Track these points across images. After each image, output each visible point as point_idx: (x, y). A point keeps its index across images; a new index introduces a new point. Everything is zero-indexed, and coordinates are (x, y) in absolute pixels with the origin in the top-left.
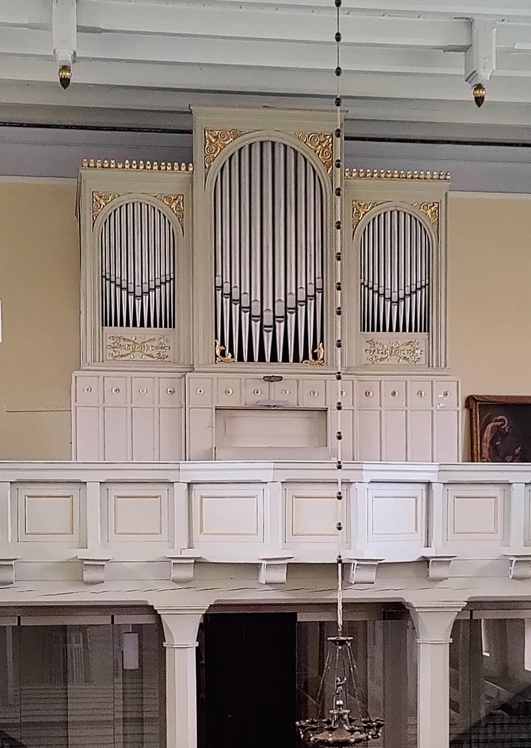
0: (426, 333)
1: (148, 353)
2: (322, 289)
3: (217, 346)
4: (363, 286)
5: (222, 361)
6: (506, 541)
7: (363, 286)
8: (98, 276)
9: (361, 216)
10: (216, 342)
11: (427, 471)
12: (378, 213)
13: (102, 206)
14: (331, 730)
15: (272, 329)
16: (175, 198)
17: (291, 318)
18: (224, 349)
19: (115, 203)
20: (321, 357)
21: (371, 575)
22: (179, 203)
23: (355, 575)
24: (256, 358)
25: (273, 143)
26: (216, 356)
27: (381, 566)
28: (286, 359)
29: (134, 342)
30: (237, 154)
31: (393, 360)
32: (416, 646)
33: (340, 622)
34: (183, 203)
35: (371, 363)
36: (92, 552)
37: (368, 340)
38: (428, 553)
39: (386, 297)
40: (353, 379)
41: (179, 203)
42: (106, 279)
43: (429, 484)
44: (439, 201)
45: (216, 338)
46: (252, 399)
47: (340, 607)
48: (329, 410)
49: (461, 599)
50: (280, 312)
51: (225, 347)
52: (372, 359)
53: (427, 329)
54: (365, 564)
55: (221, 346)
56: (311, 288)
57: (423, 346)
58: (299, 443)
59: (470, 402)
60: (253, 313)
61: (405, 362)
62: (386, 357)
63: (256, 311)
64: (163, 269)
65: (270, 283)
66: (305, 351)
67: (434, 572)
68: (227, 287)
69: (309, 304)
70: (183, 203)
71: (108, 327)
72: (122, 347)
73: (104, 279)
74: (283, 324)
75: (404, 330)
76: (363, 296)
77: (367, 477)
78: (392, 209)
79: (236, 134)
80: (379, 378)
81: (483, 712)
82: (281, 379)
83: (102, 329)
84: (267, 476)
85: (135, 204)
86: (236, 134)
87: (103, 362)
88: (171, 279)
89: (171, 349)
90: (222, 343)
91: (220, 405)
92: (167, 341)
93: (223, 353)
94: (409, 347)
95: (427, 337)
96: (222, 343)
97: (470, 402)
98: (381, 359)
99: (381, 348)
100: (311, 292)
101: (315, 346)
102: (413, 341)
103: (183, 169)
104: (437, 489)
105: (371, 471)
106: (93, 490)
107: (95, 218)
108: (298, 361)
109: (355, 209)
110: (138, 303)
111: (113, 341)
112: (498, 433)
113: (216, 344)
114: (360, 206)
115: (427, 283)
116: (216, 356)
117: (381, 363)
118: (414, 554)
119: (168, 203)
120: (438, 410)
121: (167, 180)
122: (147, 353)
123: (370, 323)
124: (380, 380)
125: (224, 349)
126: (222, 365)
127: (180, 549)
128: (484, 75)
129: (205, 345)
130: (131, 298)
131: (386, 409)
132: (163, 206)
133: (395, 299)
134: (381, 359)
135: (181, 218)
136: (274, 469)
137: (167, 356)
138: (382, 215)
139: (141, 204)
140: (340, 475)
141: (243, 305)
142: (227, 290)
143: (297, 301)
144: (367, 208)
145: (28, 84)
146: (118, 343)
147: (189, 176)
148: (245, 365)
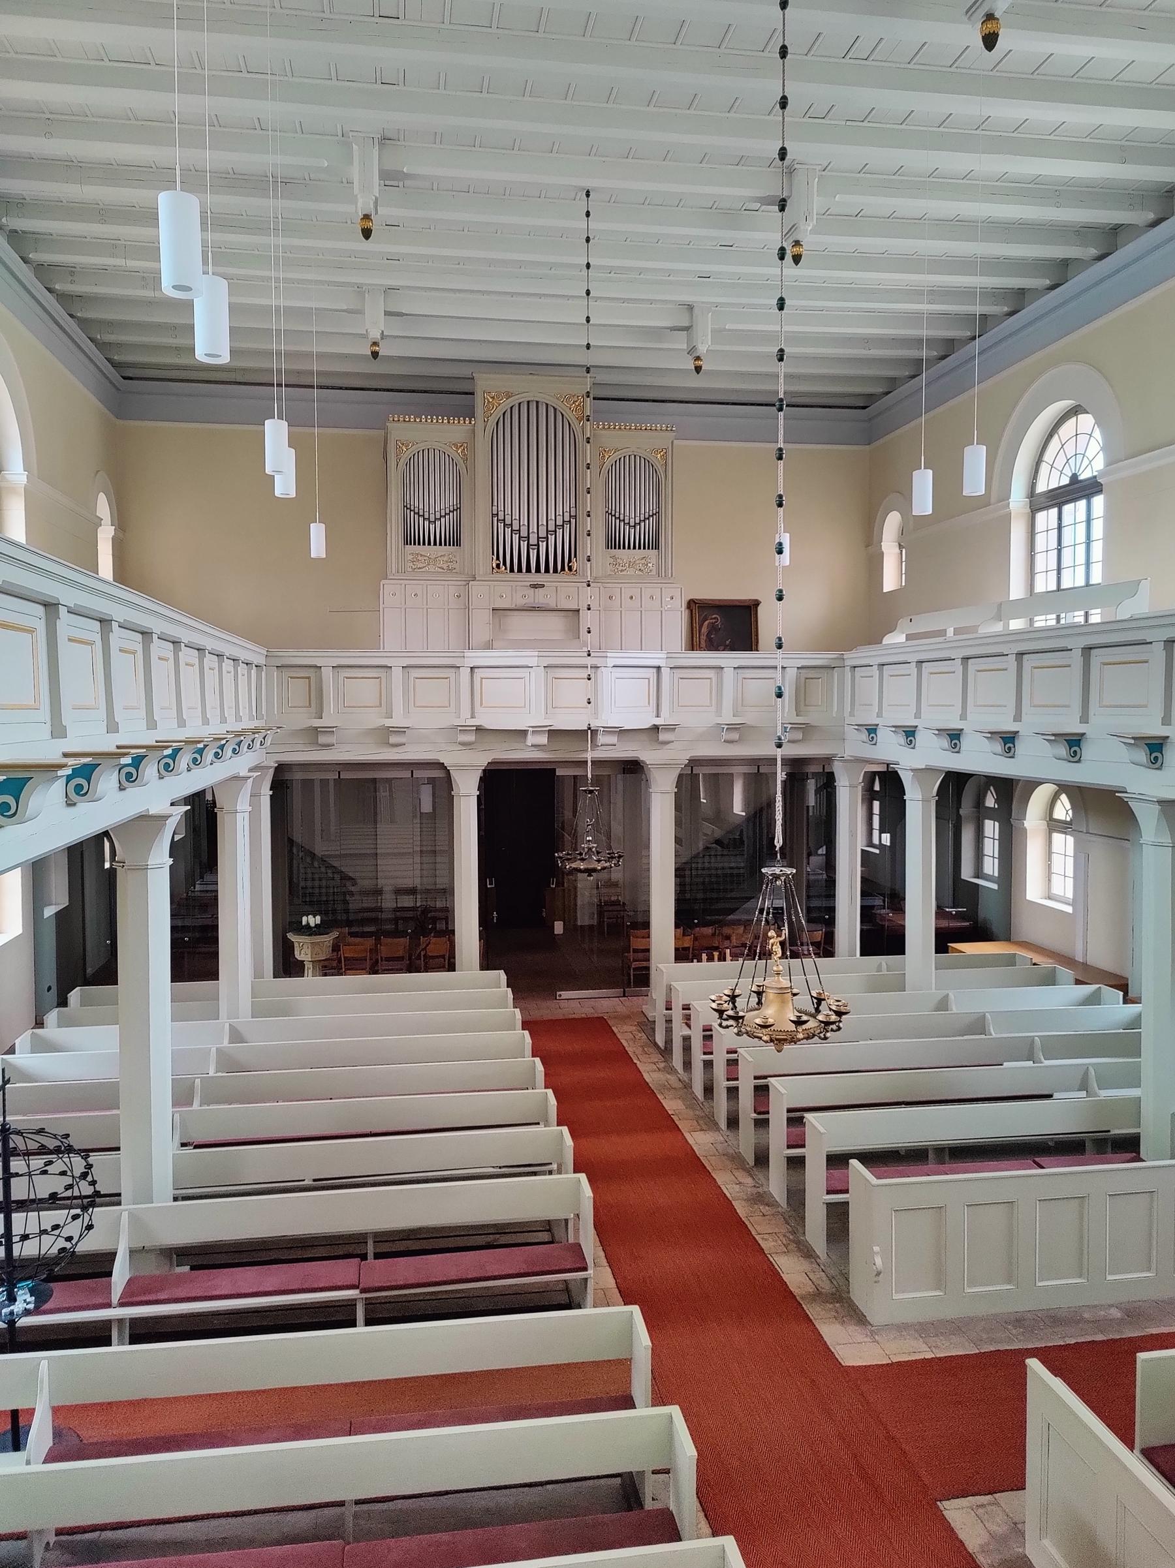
6: (719, 712)
8: (401, 506)
11: (657, 658)
14: (583, 860)
17: (551, 538)
21: (613, 739)
23: (602, 739)
24: (524, 570)
27: (622, 732)
31: (631, 572)
32: (648, 795)
33: (590, 776)
34: (468, 447)
36: (397, 721)
38: (658, 721)
43: (659, 668)
46: (520, 602)
47: (589, 764)
49: (684, 757)
50: (543, 534)
53: (657, 548)
54: (609, 731)
57: (654, 561)
58: (557, 636)
59: (691, 604)
63: (524, 533)
64: (452, 501)
65: (536, 512)
66: (563, 564)
67: (663, 736)
70: (468, 447)
76: (607, 521)
77: (611, 662)
81: (701, 846)
84: (533, 662)
90: (498, 558)
91: (496, 606)
96: (498, 558)
97: (691, 604)
100: (567, 519)
101: (570, 561)
104: (665, 672)
105: (614, 657)
106: (397, 673)
112: (713, 628)
118: (646, 720)
123: (613, 543)
126: (498, 575)
127: (465, 719)
129: (484, 559)
130: (427, 523)
132: (451, 451)
140: (589, 661)
145: (346, 357)
148: (516, 575)
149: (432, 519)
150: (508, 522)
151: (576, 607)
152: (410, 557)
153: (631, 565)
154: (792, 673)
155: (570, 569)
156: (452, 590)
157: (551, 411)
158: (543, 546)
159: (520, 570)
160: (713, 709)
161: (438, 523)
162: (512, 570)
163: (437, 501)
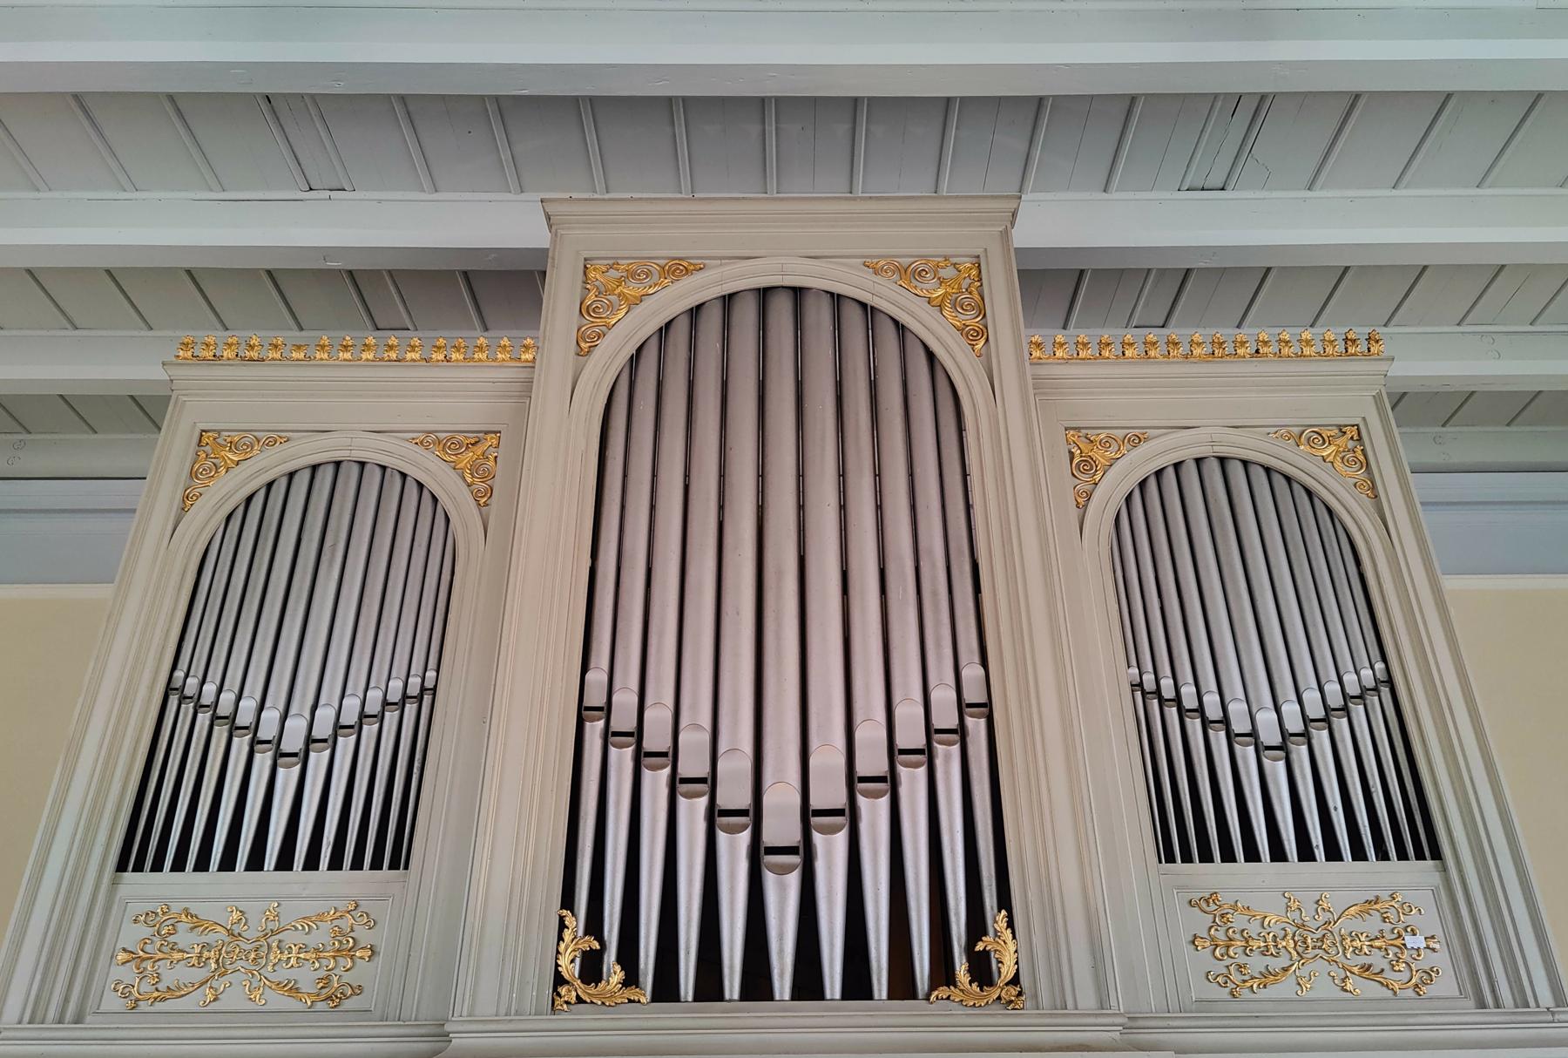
1: (283, 974)
2: (988, 705)
3: (567, 935)
5: (580, 1000)
10: (562, 919)
15: (796, 859)
17: (874, 813)
18: (596, 946)
19: (269, 464)
20: (1008, 971)
24: (732, 982)
26: (559, 980)
28: (857, 985)
29: (230, 933)
37: (1196, 896)
42: (183, 698)
44: (1358, 421)
45: (568, 901)
50: (828, 793)
51: (600, 938)
53: (1427, 846)
56: (943, 697)
57: (1428, 920)
60: (723, 802)
61: (1373, 990)
62: (1285, 970)
63: (734, 794)
69: (939, 762)
72: (177, 956)
74: (841, 839)
79: (678, 269)
83: (115, 883)
88: (423, 689)
89: (379, 960)
90: (594, 925)
92: (372, 924)
94: (1373, 924)
96: (594, 925)
98: (1267, 976)
99: (1254, 929)
100: (945, 717)
101: (977, 926)
102: (1385, 895)
108: (913, 995)
110: (287, 778)
113: (562, 926)
115: (1381, 676)
116: (559, 980)
117: (1263, 994)
122: (275, 978)
125: (596, 946)
126: (585, 1018)
133: (1270, 736)
134: (1267, 976)
135: (483, 499)
142: (624, 719)
143: (892, 751)
150: (657, 738)
152: (132, 935)
155: (982, 970)
157: (854, 320)
158: (831, 850)
162: (666, 989)
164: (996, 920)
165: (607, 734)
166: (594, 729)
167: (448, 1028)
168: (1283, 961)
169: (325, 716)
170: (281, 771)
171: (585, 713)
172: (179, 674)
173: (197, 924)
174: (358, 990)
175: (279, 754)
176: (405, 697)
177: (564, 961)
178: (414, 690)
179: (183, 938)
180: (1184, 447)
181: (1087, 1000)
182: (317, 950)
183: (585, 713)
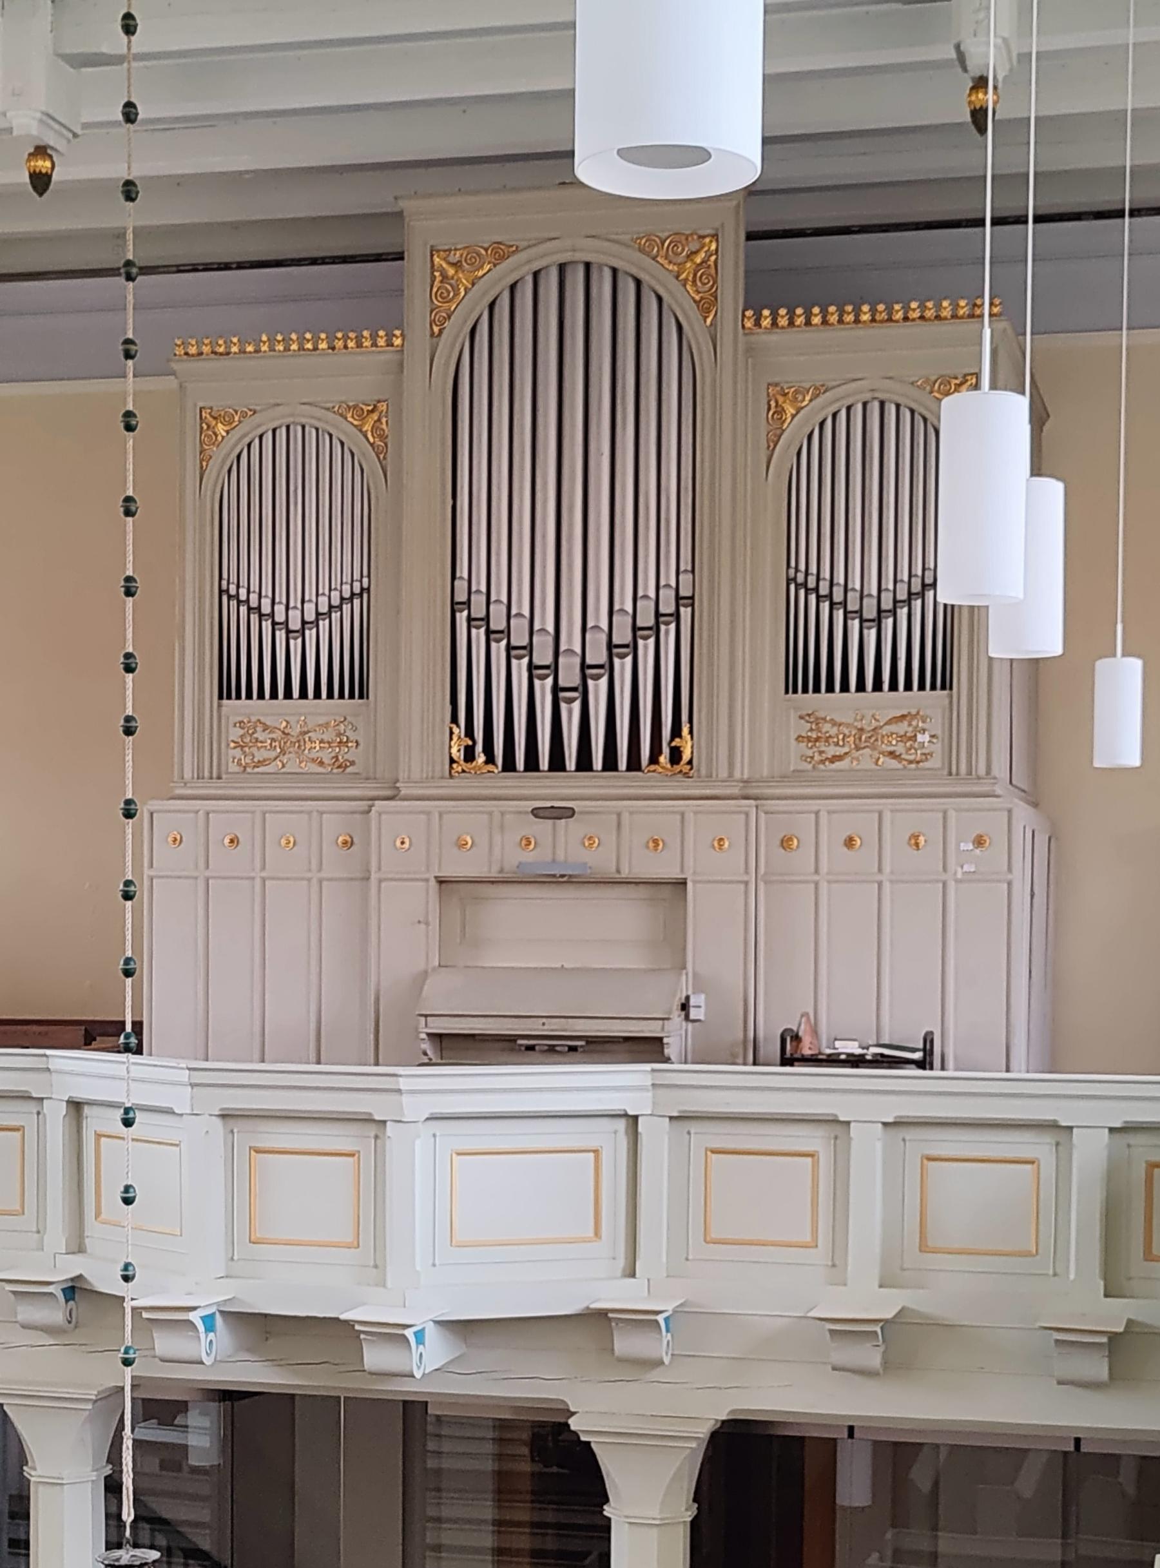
0: (945, 692)
1: (313, 755)
2: (692, 598)
3: (455, 738)
4: (792, 587)
5: (463, 771)
7: (792, 587)
9: (789, 420)
10: (451, 729)
12: (833, 409)
13: (220, 438)
16: (370, 408)
18: (470, 743)
19: (247, 429)
22: (379, 420)
24: (544, 762)
25: (588, 266)
26: (452, 761)
29: (283, 732)
30: (506, 296)
31: (866, 760)
35: (810, 767)
39: (850, 608)
40: (746, 809)
41: (379, 420)
42: (230, 597)
45: (455, 719)
46: (515, 858)
48: (690, 885)
52: (812, 758)
55: (466, 735)
56: (667, 596)
57: (936, 725)
58: (630, 959)
61: (894, 764)
62: (846, 754)
64: (345, 571)
66: (654, 744)
68: (478, 602)
70: (377, 416)
71: (233, 702)
72: (260, 745)
73: (225, 598)
75: (908, 687)
78: (867, 396)
79: (500, 252)
80: (814, 805)
82: (570, 813)
83: (220, 706)
85: (292, 428)
86: (500, 252)
87: (219, 778)
88: (362, 589)
89: (361, 747)
90: (470, 732)
93: (469, 755)
94: (903, 728)
95: (947, 701)
96: (470, 732)
100: (667, 607)
101: (676, 732)
103: (381, 342)
107: (204, 464)
109: (773, 404)
110: (296, 645)
111: (242, 732)
113: (451, 733)
114: (785, 395)
116: (452, 761)
119: (356, 423)
120: (957, 881)
121: (349, 371)
123: (806, 674)
124: (815, 808)
125: (470, 743)
128: (989, 56)
130: (281, 635)
131: (830, 877)
136: (193, 1085)
137: (353, 763)
138: (843, 413)
139: (303, 427)
141: (514, 643)
144: (804, 400)
146: (251, 735)
147: (397, 357)
149: (295, 625)
151: (674, 873)
152: (235, 733)
153: (865, 738)
154: (1091, 1150)
155: (676, 755)
156: (334, 826)
158: (598, 689)
159: (532, 764)
160: (819, 1256)
161: (311, 634)
162: (509, 765)
163: (305, 576)
164: (685, 730)
165: (470, 619)
166: (462, 617)
167: (398, 785)
168: (846, 749)
169: (310, 608)
170: (292, 642)
171: (456, 607)
172: (224, 583)
173: (266, 728)
174: (353, 763)
175: (288, 632)
176: (353, 594)
177: (454, 750)
178: (357, 590)
179: (260, 735)
180: (855, 393)
181: (724, 774)
182: (329, 743)
183: (456, 607)
